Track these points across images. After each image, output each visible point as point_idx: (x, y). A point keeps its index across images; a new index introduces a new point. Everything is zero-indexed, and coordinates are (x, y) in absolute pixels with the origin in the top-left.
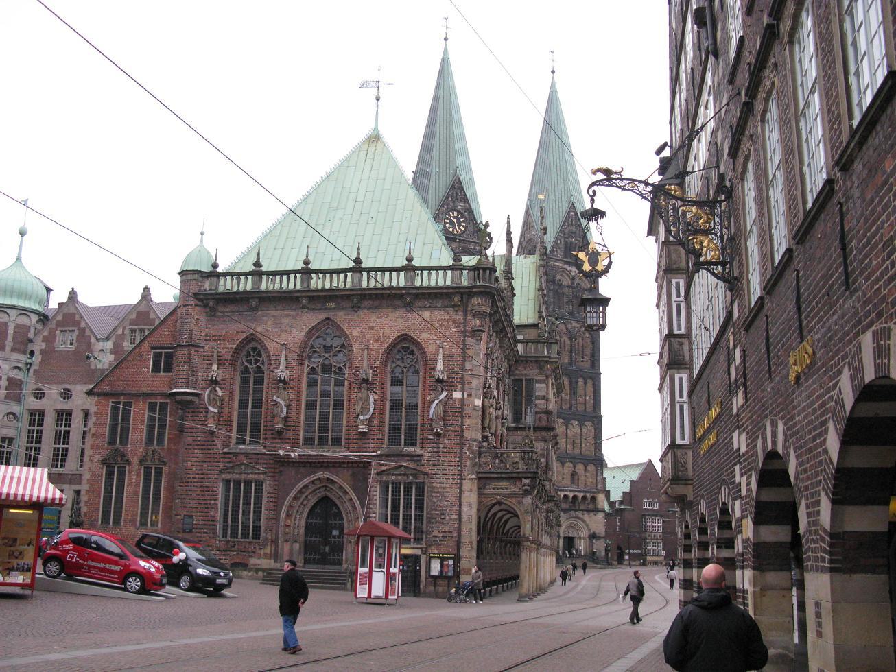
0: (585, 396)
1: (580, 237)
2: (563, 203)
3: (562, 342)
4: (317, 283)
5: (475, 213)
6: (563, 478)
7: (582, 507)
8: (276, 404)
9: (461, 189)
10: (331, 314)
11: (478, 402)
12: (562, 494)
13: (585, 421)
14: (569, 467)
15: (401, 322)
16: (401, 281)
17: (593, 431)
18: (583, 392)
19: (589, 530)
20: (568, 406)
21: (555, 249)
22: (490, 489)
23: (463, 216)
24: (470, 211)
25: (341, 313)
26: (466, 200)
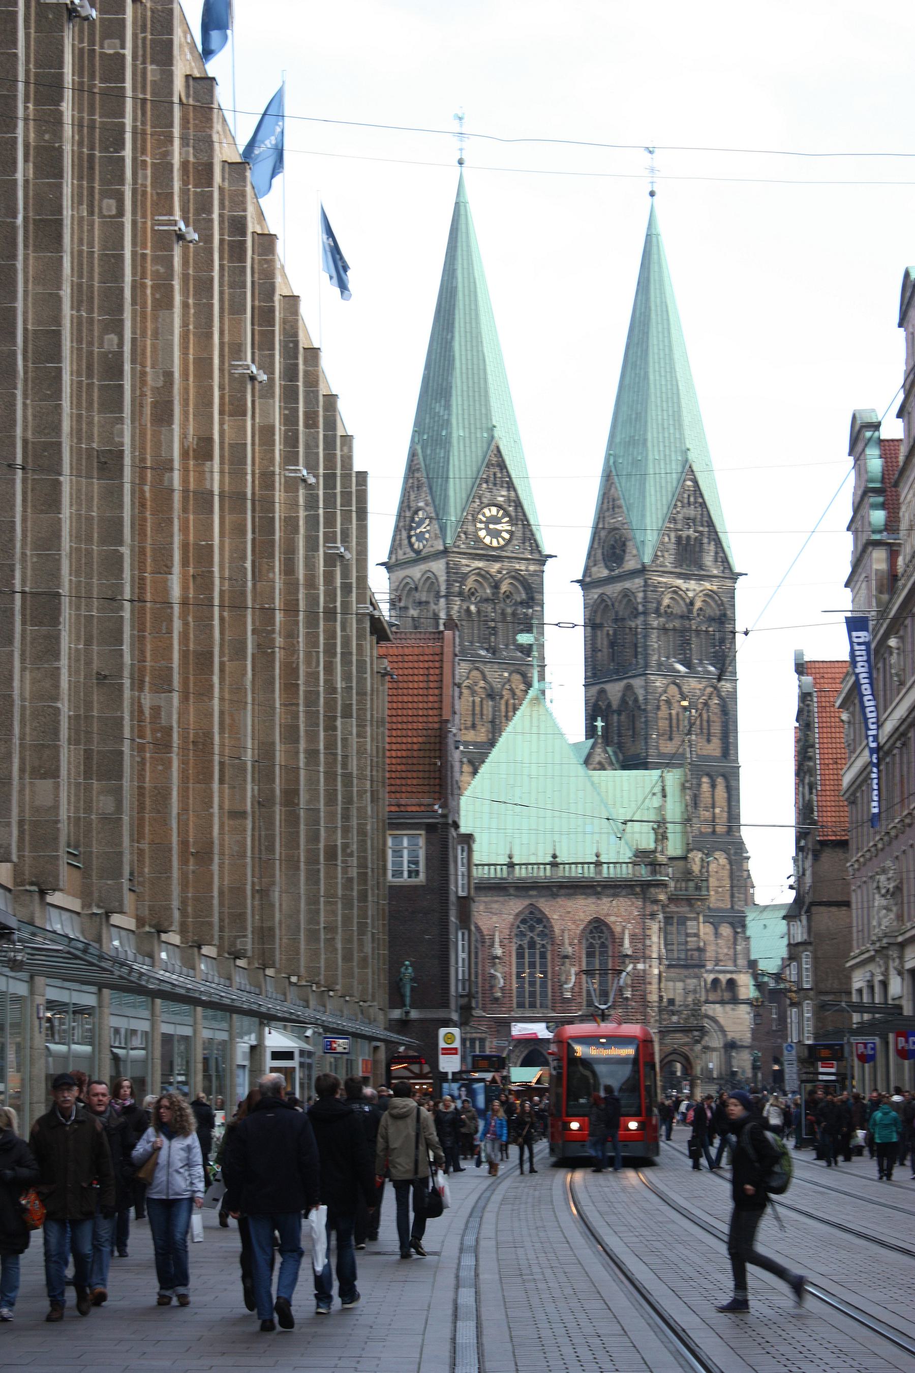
0: (713, 807)
3: (674, 717)
4: (520, 873)
8: (493, 977)
9: (502, 466)
10: (533, 901)
11: (656, 971)
15: (593, 907)
16: (590, 872)
17: (728, 867)
18: (710, 801)
19: (725, 1035)
22: (668, 1041)
24: (518, 504)
25: (542, 900)
26: (511, 486)
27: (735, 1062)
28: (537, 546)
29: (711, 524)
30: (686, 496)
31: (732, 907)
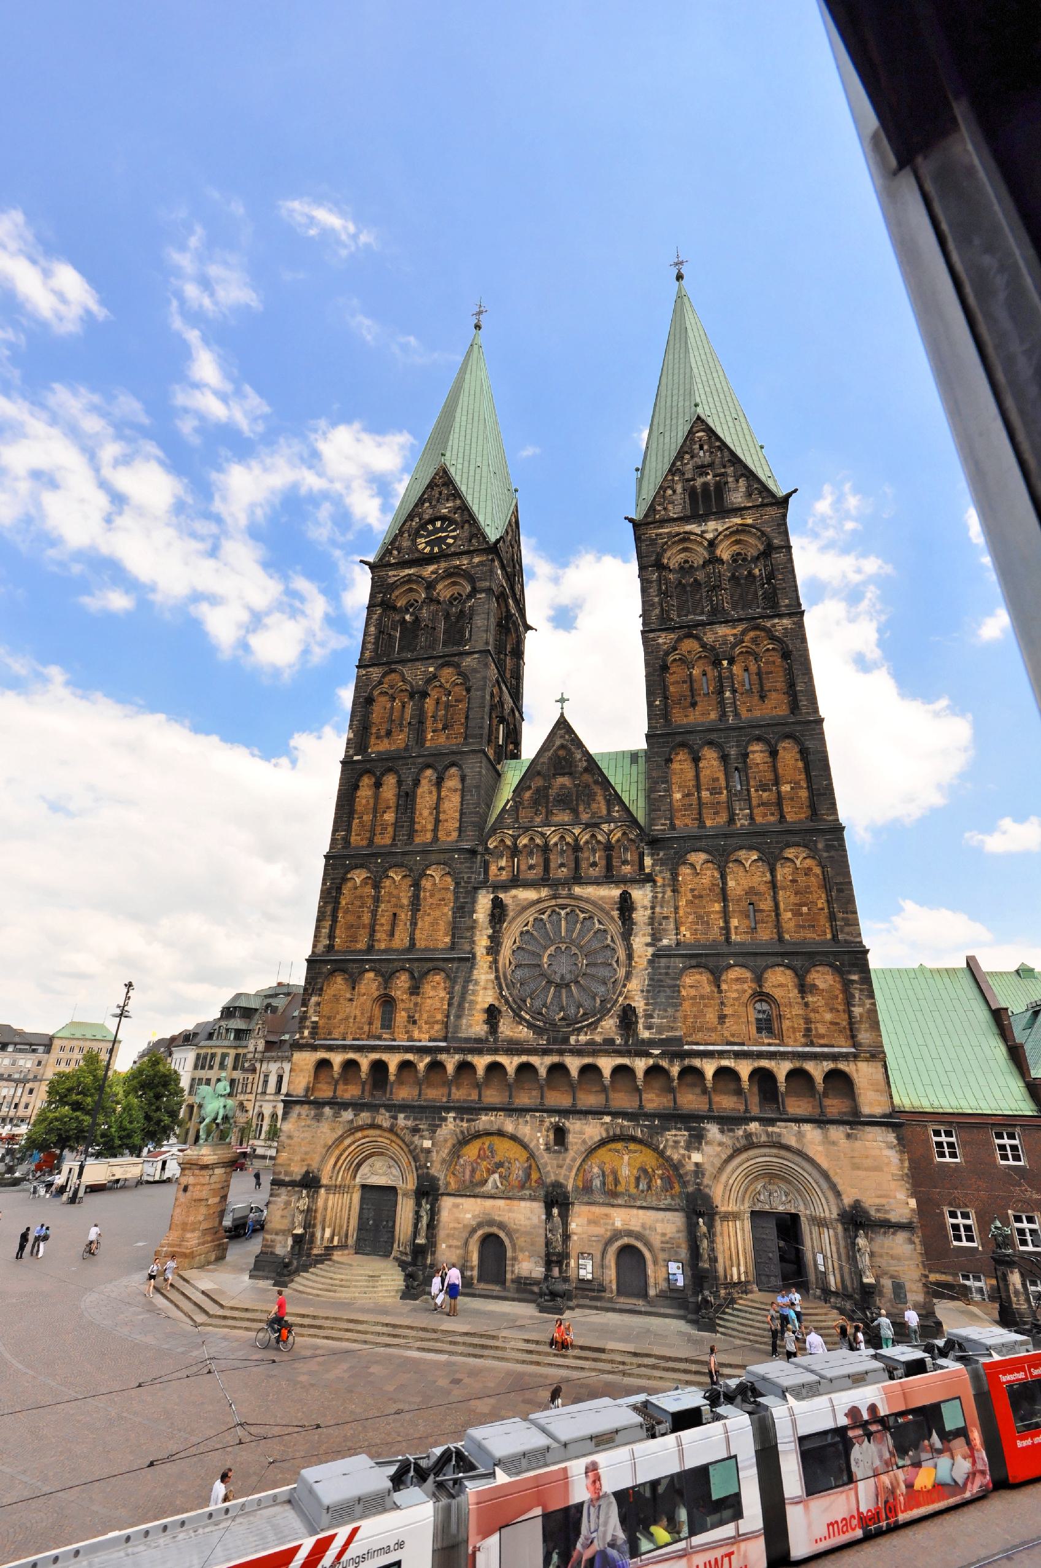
0: (777, 782)
1: (724, 467)
2: (680, 428)
5: (475, 509)
6: (722, 1018)
7: (796, 1106)
12: (709, 1068)
13: (788, 846)
14: (737, 979)
17: (817, 870)
18: (772, 777)
20: (723, 818)
21: (659, 508)
23: (452, 522)
24: (465, 508)
26: (457, 495)
27: (865, 1261)
28: (485, 538)
29: (735, 460)
30: (697, 446)
31: (835, 937)
